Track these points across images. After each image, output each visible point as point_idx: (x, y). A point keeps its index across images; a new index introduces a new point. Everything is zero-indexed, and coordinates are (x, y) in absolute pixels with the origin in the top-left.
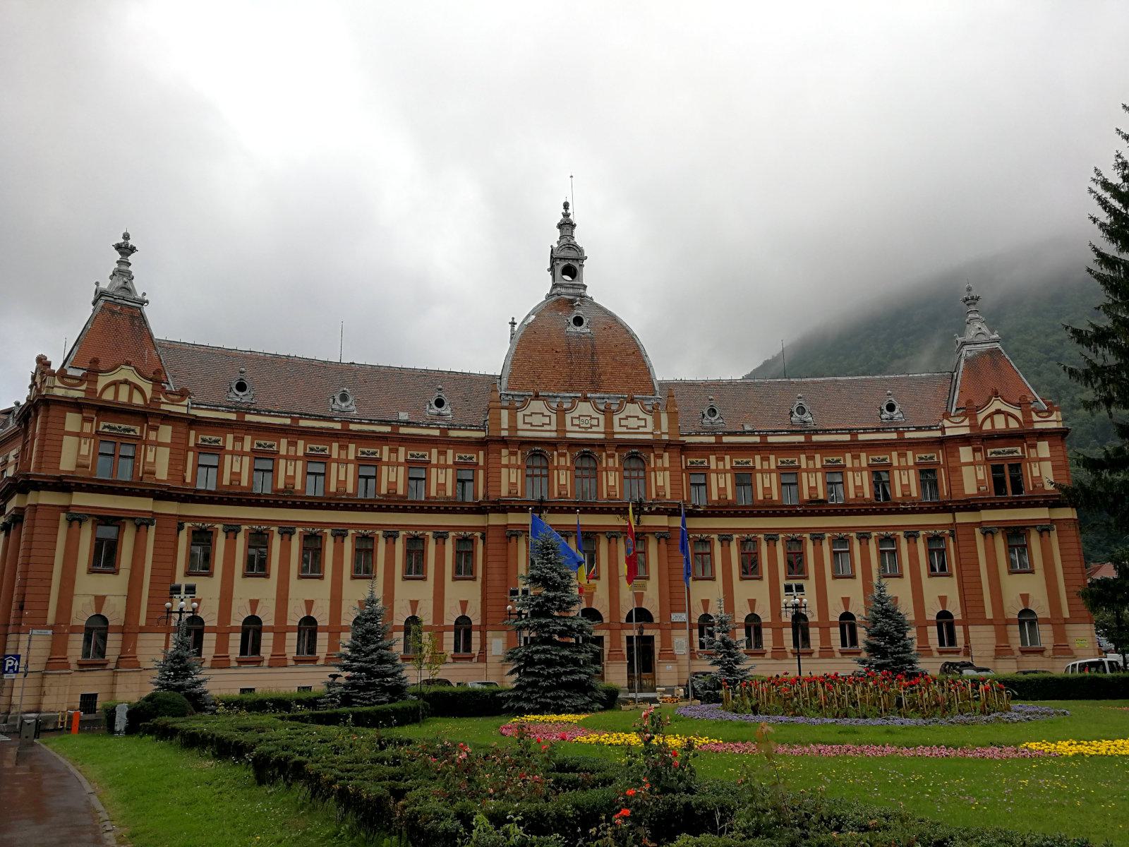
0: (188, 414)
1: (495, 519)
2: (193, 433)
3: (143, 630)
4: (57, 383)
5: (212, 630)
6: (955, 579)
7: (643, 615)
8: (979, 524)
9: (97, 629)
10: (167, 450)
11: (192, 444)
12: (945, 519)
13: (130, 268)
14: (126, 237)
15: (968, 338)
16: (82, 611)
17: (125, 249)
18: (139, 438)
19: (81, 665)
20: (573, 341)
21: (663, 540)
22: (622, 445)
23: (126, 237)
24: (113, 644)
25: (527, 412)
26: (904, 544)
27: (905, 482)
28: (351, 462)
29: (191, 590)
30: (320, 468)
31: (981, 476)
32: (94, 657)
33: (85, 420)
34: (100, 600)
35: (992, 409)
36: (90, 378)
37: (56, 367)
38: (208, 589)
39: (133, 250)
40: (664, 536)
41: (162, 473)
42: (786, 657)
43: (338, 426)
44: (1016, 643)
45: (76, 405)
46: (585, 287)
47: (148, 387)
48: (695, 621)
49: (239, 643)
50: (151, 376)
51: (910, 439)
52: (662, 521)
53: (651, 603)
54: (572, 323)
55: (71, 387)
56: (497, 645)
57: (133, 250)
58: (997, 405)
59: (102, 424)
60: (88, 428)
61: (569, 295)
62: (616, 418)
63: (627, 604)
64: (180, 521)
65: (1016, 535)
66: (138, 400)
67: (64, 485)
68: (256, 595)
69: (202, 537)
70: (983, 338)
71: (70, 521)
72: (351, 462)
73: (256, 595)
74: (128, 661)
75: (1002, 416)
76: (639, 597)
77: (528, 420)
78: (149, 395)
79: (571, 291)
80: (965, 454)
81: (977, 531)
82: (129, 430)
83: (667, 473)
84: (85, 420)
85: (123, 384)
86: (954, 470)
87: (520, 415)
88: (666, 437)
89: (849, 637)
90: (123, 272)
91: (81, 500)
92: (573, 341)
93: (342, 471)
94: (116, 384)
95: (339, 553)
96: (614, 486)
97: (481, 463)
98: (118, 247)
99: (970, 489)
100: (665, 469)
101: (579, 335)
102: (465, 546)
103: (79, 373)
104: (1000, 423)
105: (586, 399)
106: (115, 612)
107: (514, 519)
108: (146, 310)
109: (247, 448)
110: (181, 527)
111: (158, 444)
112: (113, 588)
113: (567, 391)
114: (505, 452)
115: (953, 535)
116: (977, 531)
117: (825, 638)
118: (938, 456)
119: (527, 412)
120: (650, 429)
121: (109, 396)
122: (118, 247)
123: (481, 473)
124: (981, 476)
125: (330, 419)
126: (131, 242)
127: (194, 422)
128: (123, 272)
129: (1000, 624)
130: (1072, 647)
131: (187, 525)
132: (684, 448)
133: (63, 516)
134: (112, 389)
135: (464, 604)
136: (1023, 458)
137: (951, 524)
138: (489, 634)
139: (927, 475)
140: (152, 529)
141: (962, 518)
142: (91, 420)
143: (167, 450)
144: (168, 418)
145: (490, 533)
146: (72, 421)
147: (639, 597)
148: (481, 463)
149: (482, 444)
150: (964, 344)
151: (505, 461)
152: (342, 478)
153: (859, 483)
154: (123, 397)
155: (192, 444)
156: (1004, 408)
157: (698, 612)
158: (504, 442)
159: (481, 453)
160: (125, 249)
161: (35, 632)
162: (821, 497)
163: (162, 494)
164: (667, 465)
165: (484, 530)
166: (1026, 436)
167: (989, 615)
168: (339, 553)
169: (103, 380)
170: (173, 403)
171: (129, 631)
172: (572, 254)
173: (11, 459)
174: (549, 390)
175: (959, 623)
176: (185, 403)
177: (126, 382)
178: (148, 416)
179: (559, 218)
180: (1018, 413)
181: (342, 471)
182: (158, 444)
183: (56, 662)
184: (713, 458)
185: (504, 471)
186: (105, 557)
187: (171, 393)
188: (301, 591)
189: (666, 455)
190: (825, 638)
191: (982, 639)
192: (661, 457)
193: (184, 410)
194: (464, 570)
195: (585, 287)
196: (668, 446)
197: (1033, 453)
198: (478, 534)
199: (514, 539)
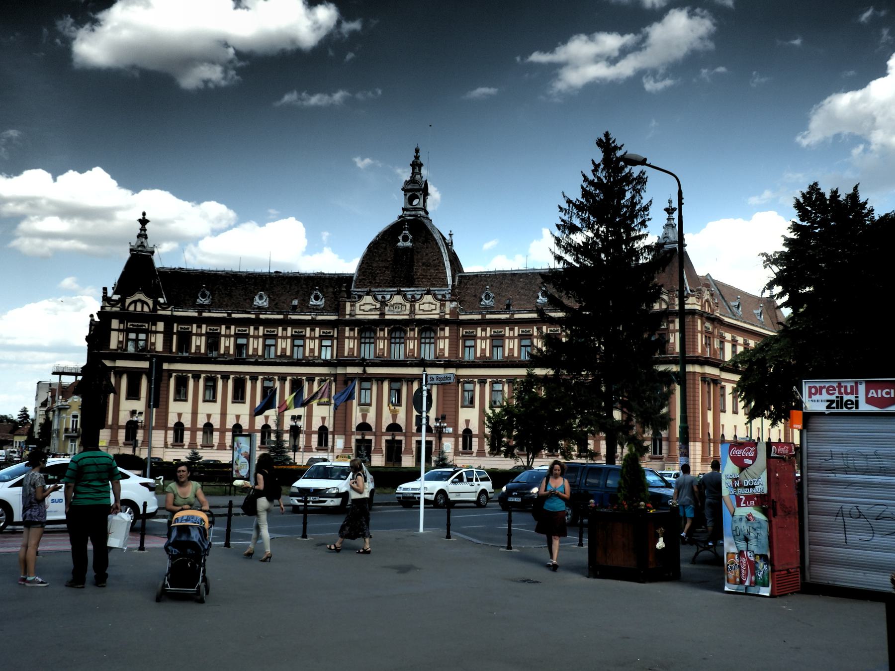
1: (340, 371)
2: (175, 325)
3: (154, 428)
5: (188, 429)
7: (394, 428)
10: (162, 335)
11: (175, 331)
16: (124, 418)
17: (144, 222)
22: (420, 322)
24: (140, 435)
25: (362, 303)
28: (261, 337)
39: (148, 221)
42: (484, 456)
43: (253, 316)
48: (460, 432)
52: (440, 371)
56: (340, 443)
57: (148, 221)
61: (410, 216)
62: (417, 305)
63: (387, 420)
66: (146, 309)
68: (210, 411)
72: (261, 337)
73: (210, 411)
77: (362, 308)
78: (151, 306)
79: (413, 213)
83: (447, 341)
87: (357, 305)
88: (447, 317)
90: (143, 235)
91: (120, 363)
93: (256, 342)
94: (135, 302)
105: (399, 293)
107: (350, 370)
109: (204, 331)
111: (156, 332)
113: (391, 287)
119: (362, 303)
120: (438, 311)
121: (132, 308)
125: (249, 313)
128: (143, 235)
131: (174, 374)
135: (323, 419)
143: (162, 335)
145: (338, 378)
151: (347, 334)
155: (175, 331)
157: (462, 427)
164: (447, 334)
165: (335, 375)
170: (164, 309)
171: (148, 429)
177: (139, 300)
181: (256, 342)
182: (156, 332)
183: (114, 442)
185: (347, 341)
188: (204, 409)
189: (447, 329)
193: (169, 313)
196: (446, 322)
199: (350, 382)
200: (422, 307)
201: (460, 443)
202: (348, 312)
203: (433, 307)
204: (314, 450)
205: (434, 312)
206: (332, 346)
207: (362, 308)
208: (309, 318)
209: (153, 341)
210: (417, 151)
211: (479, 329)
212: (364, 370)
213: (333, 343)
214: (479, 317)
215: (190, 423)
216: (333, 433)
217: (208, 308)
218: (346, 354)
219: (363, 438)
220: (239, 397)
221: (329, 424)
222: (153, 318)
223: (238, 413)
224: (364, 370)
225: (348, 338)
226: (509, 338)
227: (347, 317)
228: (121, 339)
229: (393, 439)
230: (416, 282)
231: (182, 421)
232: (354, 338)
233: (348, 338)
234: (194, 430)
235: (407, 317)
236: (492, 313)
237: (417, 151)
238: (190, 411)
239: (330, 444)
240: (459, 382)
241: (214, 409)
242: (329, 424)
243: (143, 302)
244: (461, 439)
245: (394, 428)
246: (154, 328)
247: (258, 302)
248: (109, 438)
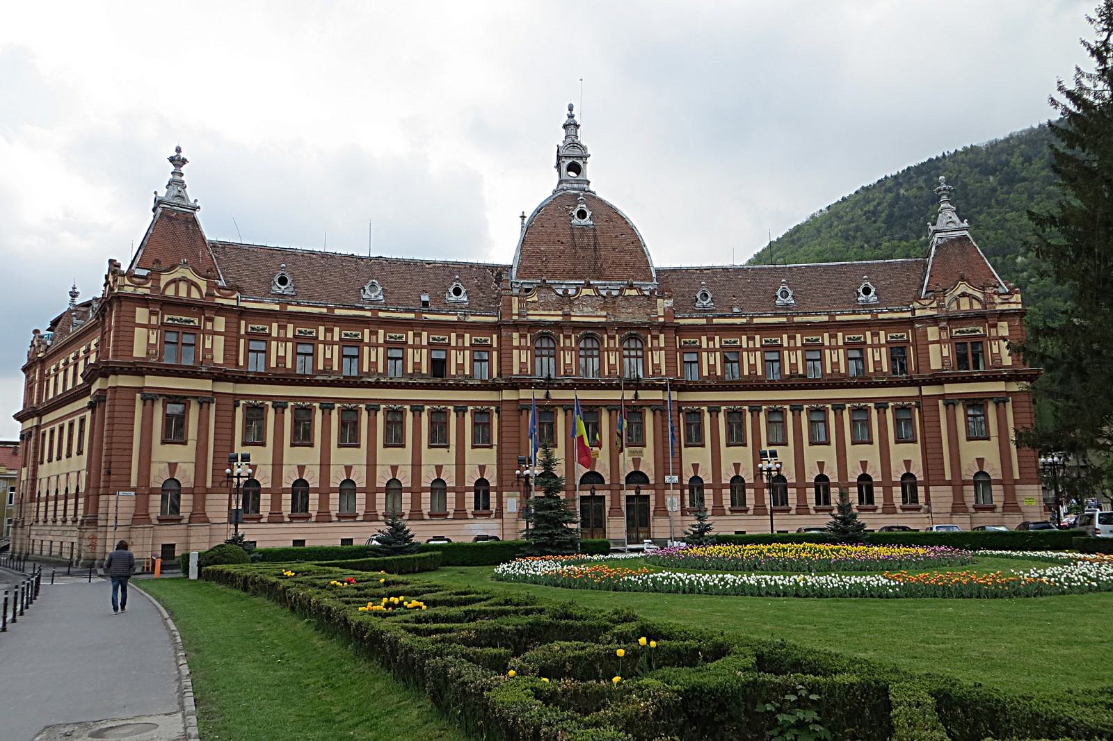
0: (237, 306)
1: (507, 395)
2: (243, 323)
4: (127, 282)
5: (267, 491)
6: (919, 445)
7: (637, 477)
8: (942, 396)
9: (172, 490)
11: (243, 332)
12: (912, 392)
13: (183, 178)
14: (178, 150)
15: (939, 226)
16: (158, 475)
17: (178, 161)
18: (198, 328)
19: (160, 520)
20: (579, 235)
21: (658, 412)
23: (178, 150)
24: (186, 503)
27: (878, 358)
29: (246, 458)
31: (945, 353)
32: (171, 515)
33: (152, 313)
34: (173, 467)
35: (958, 292)
36: (154, 276)
37: (124, 268)
38: (262, 457)
39: (184, 161)
40: (659, 408)
41: (219, 358)
43: (368, 314)
44: (970, 500)
45: (143, 301)
46: (588, 182)
47: (203, 284)
48: (686, 482)
49: (290, 502)
50: (205, 273)
51: (883, 319)
52: (658, 395)
53: (648, 466)
54: (576, 216)
55: (139, 285)
56: (512, 503)
57: (184, 161)
58: (962, 288)
60: (154, 320)
61: (574, 189)
63: (626, 467)
64: (236, 399)
65: (976, 403)
66: (195, 295)
67: (138, 369)
68: (302, 461)
69: (255, 413)
70: (953, 226)
71: (144, 400)
73: (302, 461)
74: (198, 516)
75: (966, 299)
76: (636, 462)
78: (204, 291)
79: (576, 186)
81: (940, 402)
82: (189, 321)
84: (152, 313)
85: (182, 282)
86: (922, 346)
88: (661, 320)
89: (823, 498)
90: (176, 182)
91: (151, 381)
92: (579, 235)
93: (373, 353)
94: (174, 281)
96: (571, 364)
97: (495, 345)
98: (172, 160)
99: (935, 364)
100: (661, 349)
101: (583, 229)
103: (144, 273)
104: (965, 305)
105: (589, 286)
106: (186, 475)
107: (524, 394)
108: (198, 215)
110: (236, 405)
112: (183, 455)
113: (571, 278)
114: (515, 335)
116: (940, 402)
117: (802, 497)
121: (170, 292)
122: (172, 160)
123: (495, 353)
124: (945, 353)
125: (362, 309)
126: (183, 155)
127: (243, 313)
128: (176, 182)
129: (958, 484)
130: (1020, 504)
132: (679, 329)
133: (138, 396)
134: (173, 286)
135: (482, 468)
137: (918, 396)
138: (505, 494)
139: (897, 353)
140: (213, 407)
141: (926, 390)
142: (156, 314)
144: (221, 310)
145: (504, 407)
146: (141, 315)
147: (636, 462)
148: (495, 345)
149: (496, 327)
150: (936, 232)
151: (516, 343)
153: (419, 359)
154: (183, 293)
156: (970, 291)
157: (688, 475)
158: (516, 326)
159: (495, 336)
161: (121, 493)
162: (801, 372)
163: (219, 376)
164: (662, 345)
165: (499, 404)
166: (987, 317)
167: (948, 477)
169: (165, 279)
170: (225, 297)
171: (199, 492)
172: (577, 152)
173: (93, 347)
174: (556, 278)
175: (921, 484)
176: (234, 297)
177: (184, 279)
178: (205, 308)
179: (565, 119)
180: (979, 295)
181: (373, 353)
183: (140, 517)
184: (704, 338)
185: (515, 352)
186: (175, 431)
187: (223, 288)
190: (802, 497)
191: (942, 496)
192: (657, 338)
193: (234, 303)
194: (481, 441)
195: (588, 182)
196: (663, 328)
198: (493, 408)
199: (524, 412)
201: (687, 497)
202: (515, 311)
204: (470, 516)
206: (489, 361)
208: (455, 318)
209: (208, 346)
210: (571, 109)
212: (547, 395)
213: (491, 356)
214: (704, 321)
217: (294, 298)
218: (516, 371)
219: (593, 494)
220: (349, 436)
221: (492, 478)
222: (205, 308)
223: (394, 463)
224: (547, 395)
225: (517, 348)
227: (515, 318)
228: (152, 341)
229: (593, 494)
230: (607, 272)
233: (517, 348)
235: (603, 320)
236: (720, 317)
237: (571, 109)
239: (493, 506)
240: (680, 410)
241: (310, 457)
242: (492, 478)
243: (191, 284)
244: (687, 492)
245: (637, 477)
246: (209, 326)
247: (369, 294)
248: (133, 510)
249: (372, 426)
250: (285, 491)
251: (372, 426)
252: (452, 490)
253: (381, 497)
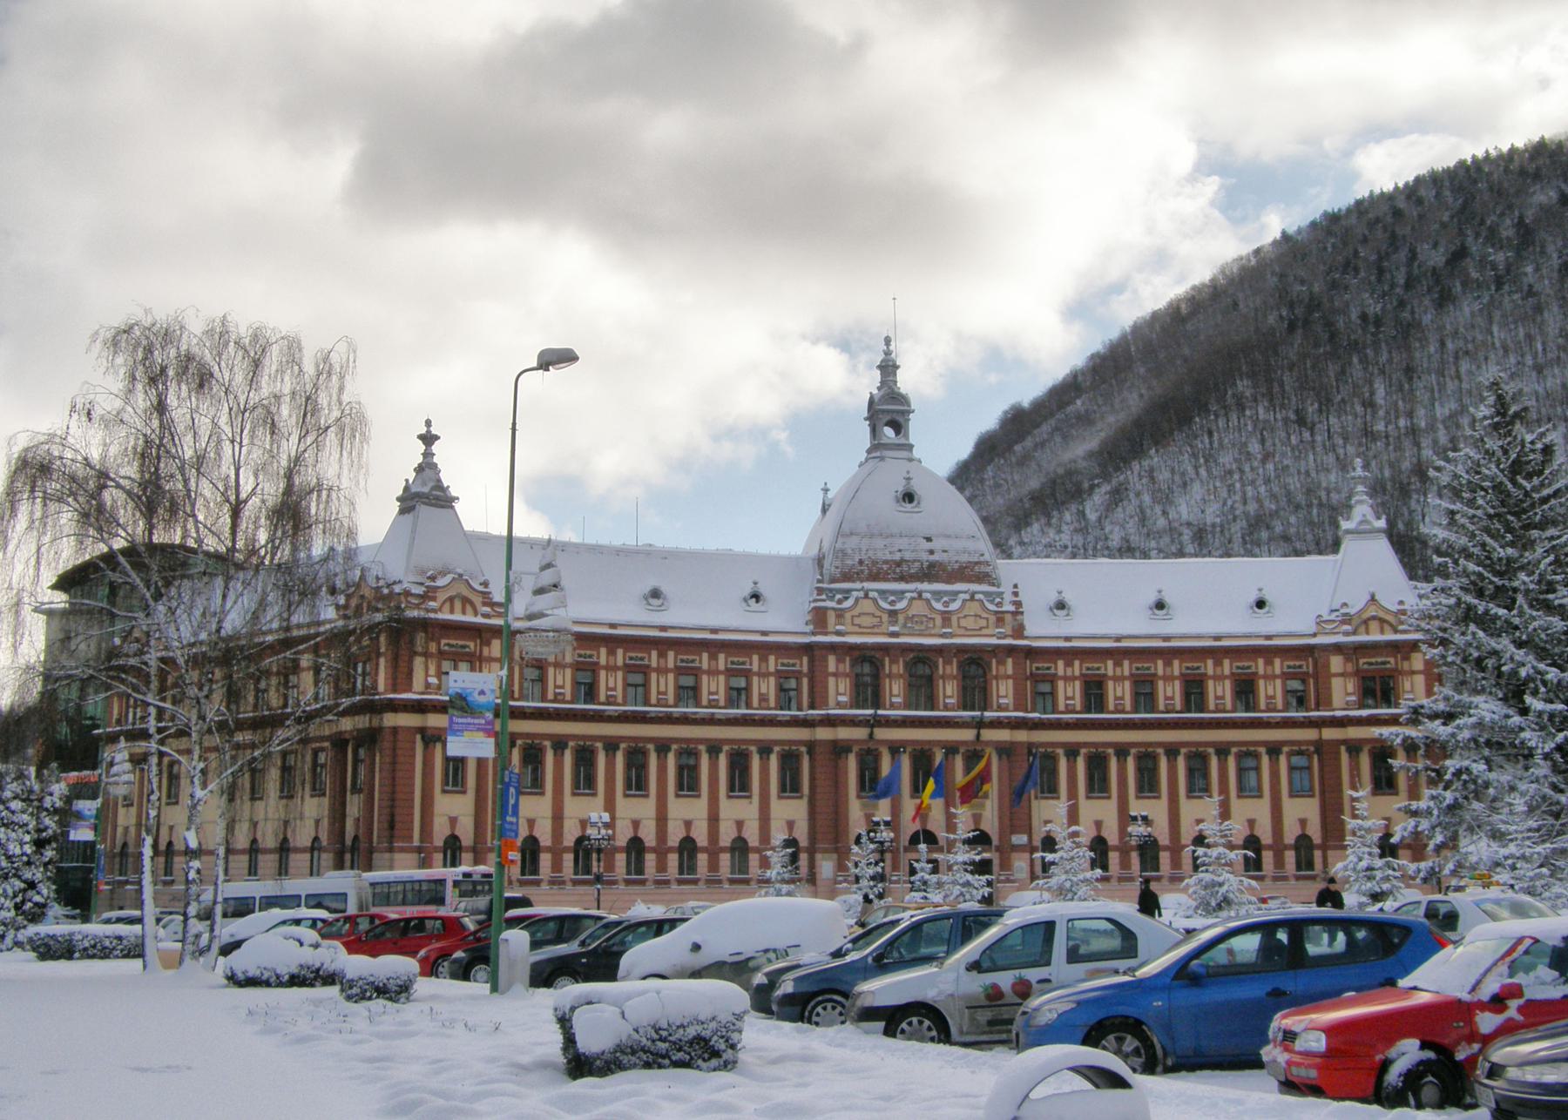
1: (823, 734)
8: (1344, 742)
12: (1310, 734)
14: (428, 423)
23: (428, 423)
26: (1265, 760)
30: (638, 679)
46: (911, 447)
52: (1003, 735)
53: (990, 824)
59: (443, 642)
76: (977, 818)
77: (857, 621)
80: (1336, 663)
83: (1010, 682)
95: (662, 769)
98: (421, 437)
100: (1008, 677)
102: (789, 761)
110: (513, 744)
115: (1318, 751)
118: (1307, 666)
123: (805, 681)
124: (1350, 688)
126: (434, 431)
131: (519, 742)
136: (1396, 670)
138: (818, 856)
141: (1329, 734)
147: (977, 818)
151: (832, 667)
152: (662, 689)
159: (805, 659)
160: (428, 439)
164: (1010, 672)
165: (811, 746)
168: (662, 769)
181: (662, 681)
185: (831, 680)
189: (1010, 661)
194: (790, 786)
195: (911, 447)
197: (1406, 666)
200: (963, 623)
203: (984, 623)
205: (985, 631)
207: (857, 621)
211: (1061, 664)
212: (871, 735)
213: (799, 684)
215: (471, 835)
216: (1324, 847)
220: (636, 784)
223: (740, 817)
225: (835, 675)
226: (1066, 679)
231: (640, 835)
232: (847, 675)
234: (661, 851)
238: (757, 816)
249: (662, 770)
250: (566, 849)
251: (558, 768)
252: (704, 850)
253: (725, 858)
